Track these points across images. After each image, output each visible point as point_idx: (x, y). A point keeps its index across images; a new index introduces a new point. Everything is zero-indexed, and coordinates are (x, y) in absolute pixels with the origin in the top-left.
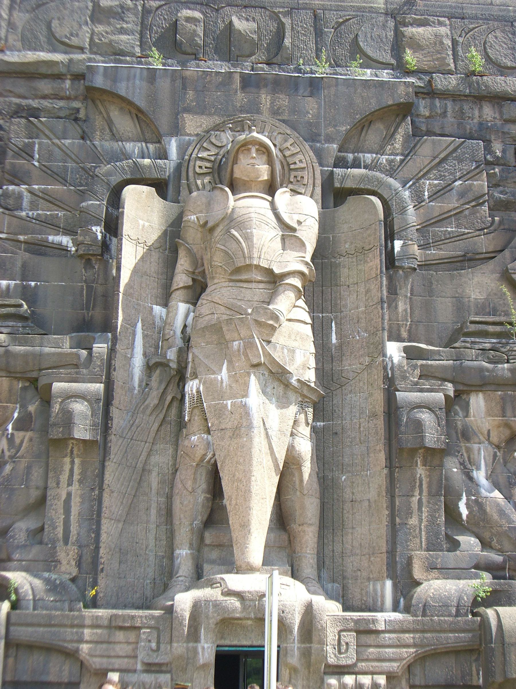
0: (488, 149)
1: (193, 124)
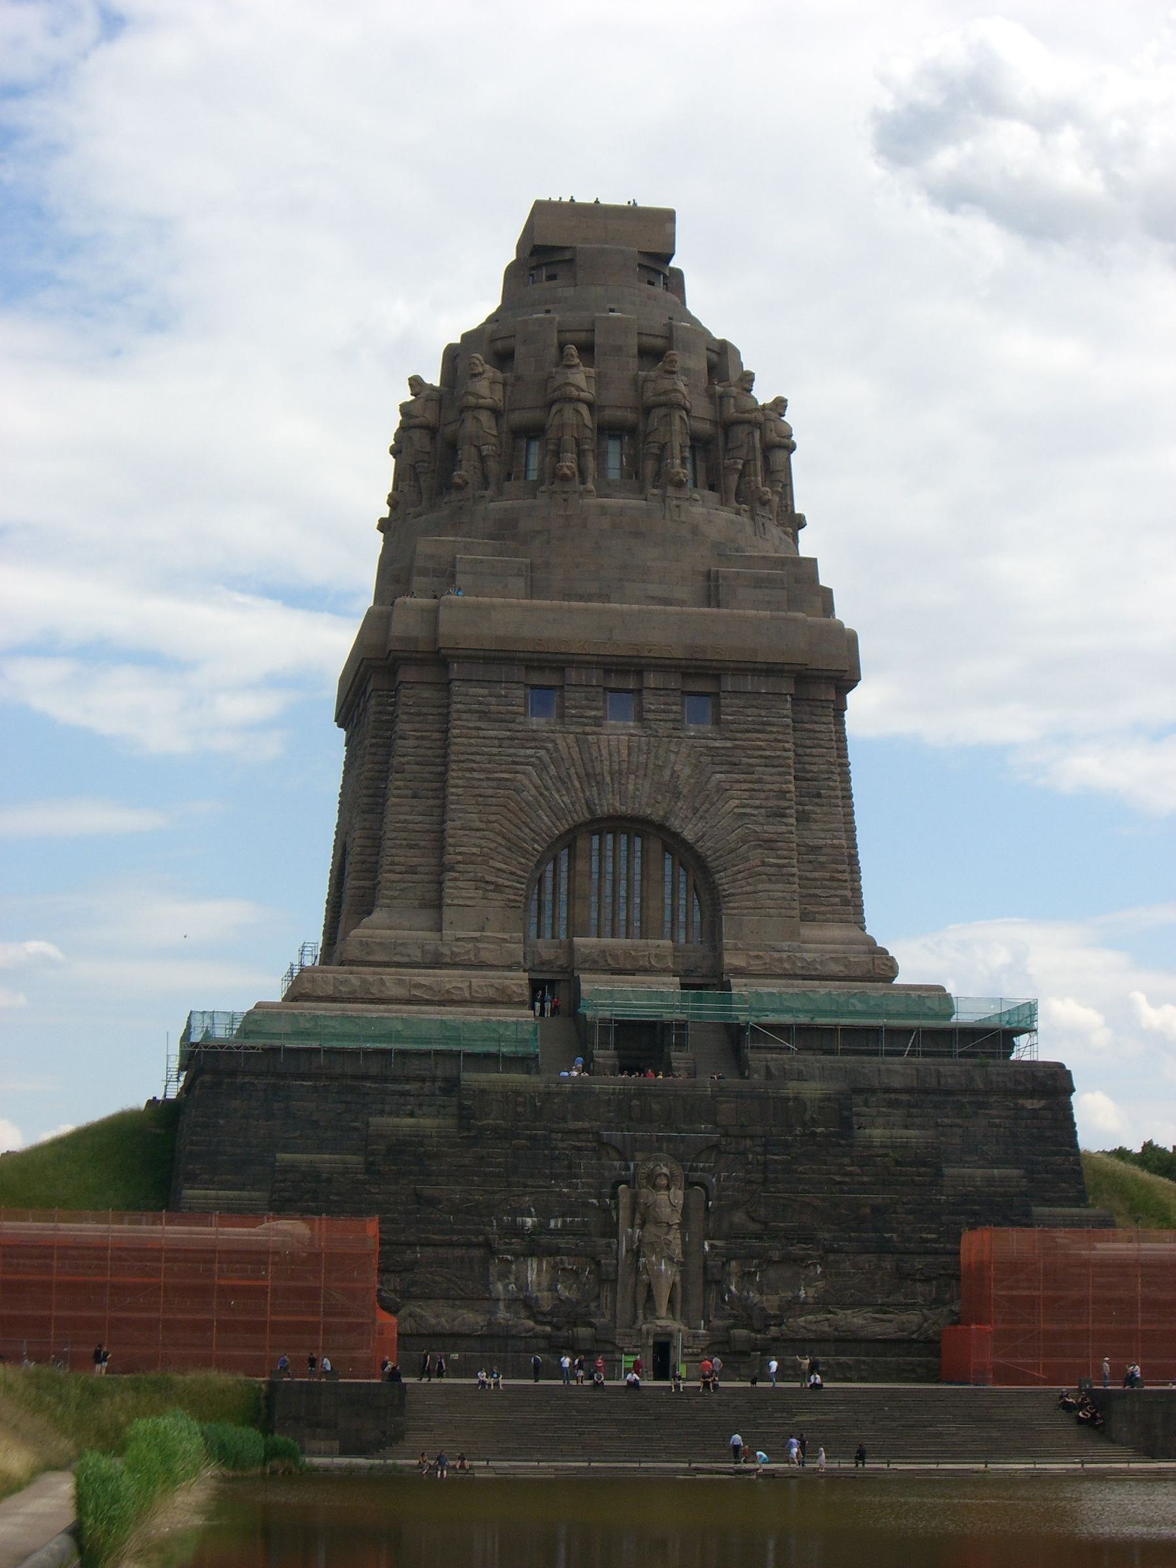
0: (747, 1158)
1: (639, 1156)
